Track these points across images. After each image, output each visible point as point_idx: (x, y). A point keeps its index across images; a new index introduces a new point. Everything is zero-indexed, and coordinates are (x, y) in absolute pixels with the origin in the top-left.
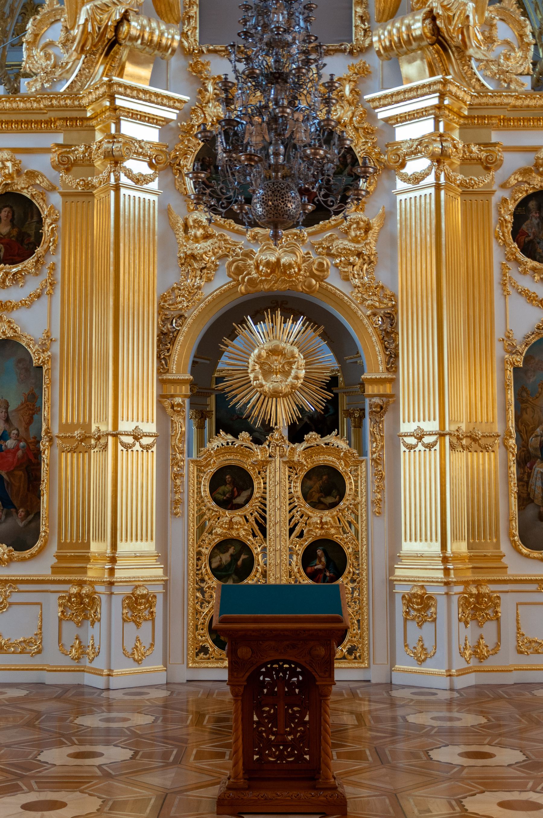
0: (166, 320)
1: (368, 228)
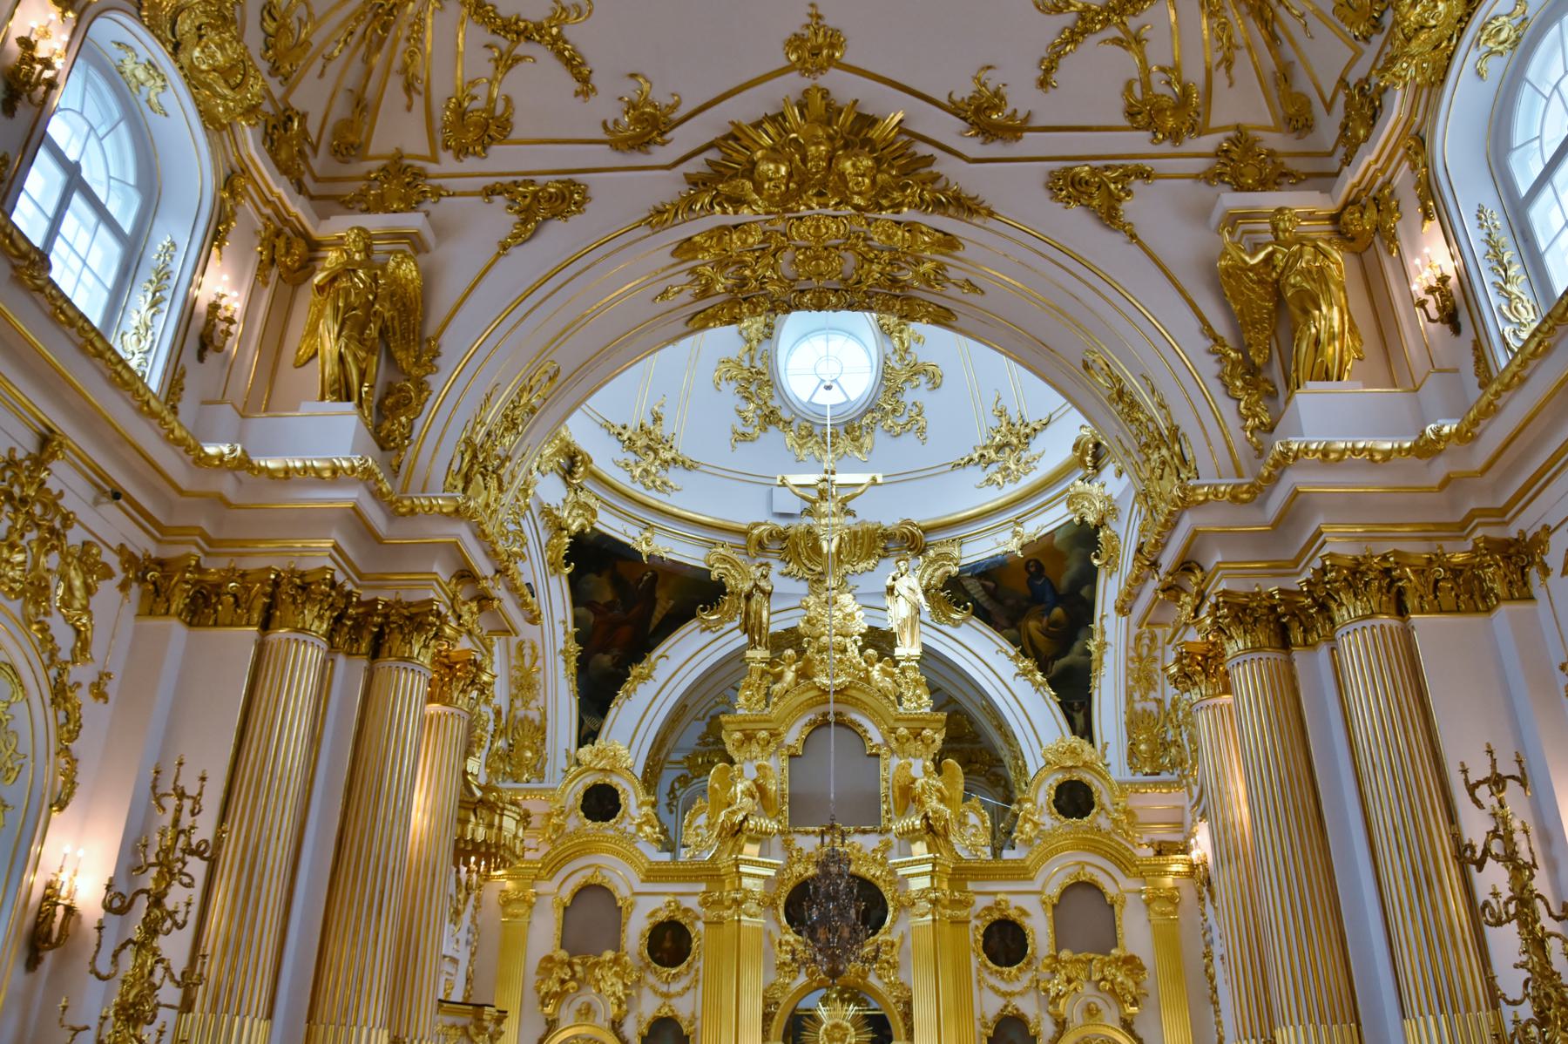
0: (767, 1005)
1: (893, 945)
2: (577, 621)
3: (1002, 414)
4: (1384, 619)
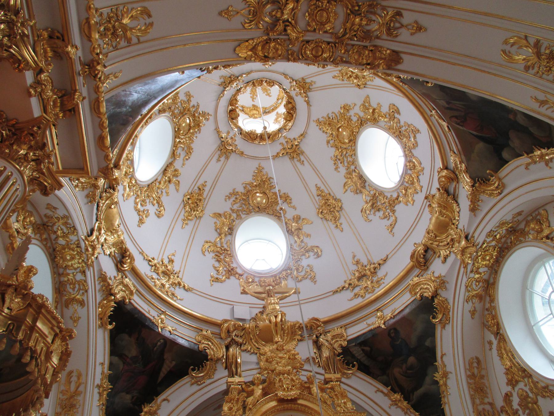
3: (358, 262)
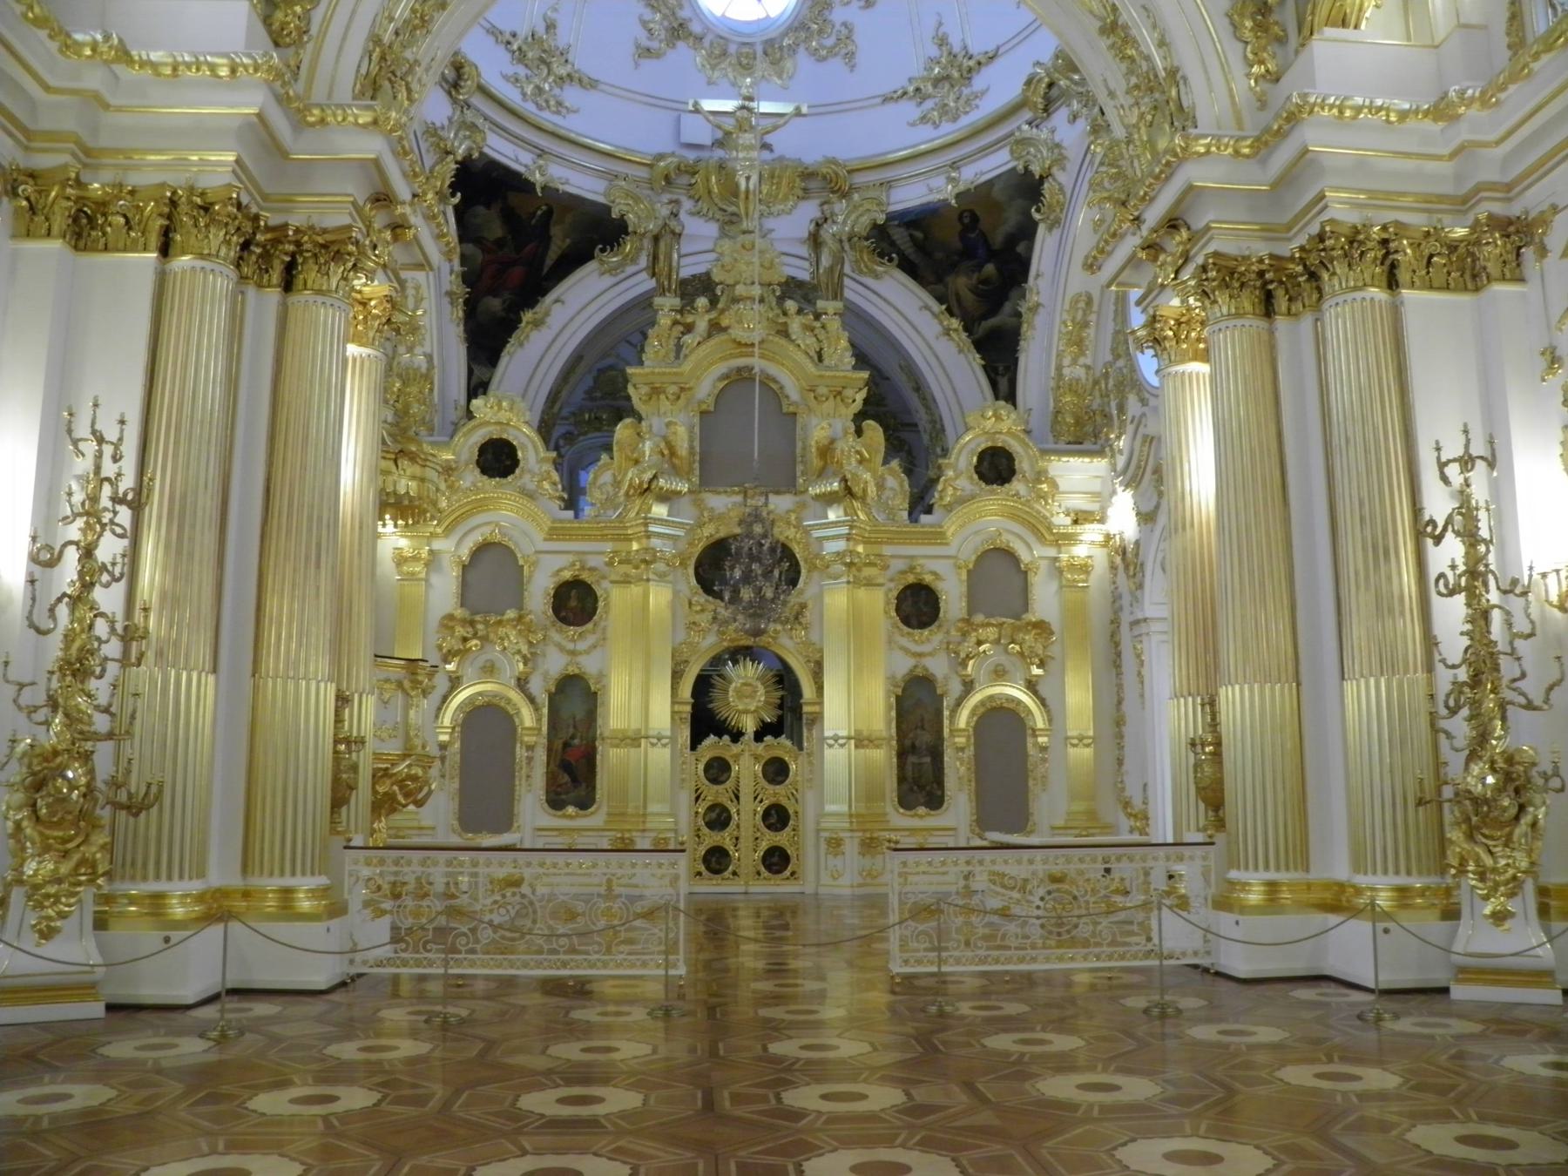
2: (464, 259)
3: (942, 42)
4: (1374, 291)
